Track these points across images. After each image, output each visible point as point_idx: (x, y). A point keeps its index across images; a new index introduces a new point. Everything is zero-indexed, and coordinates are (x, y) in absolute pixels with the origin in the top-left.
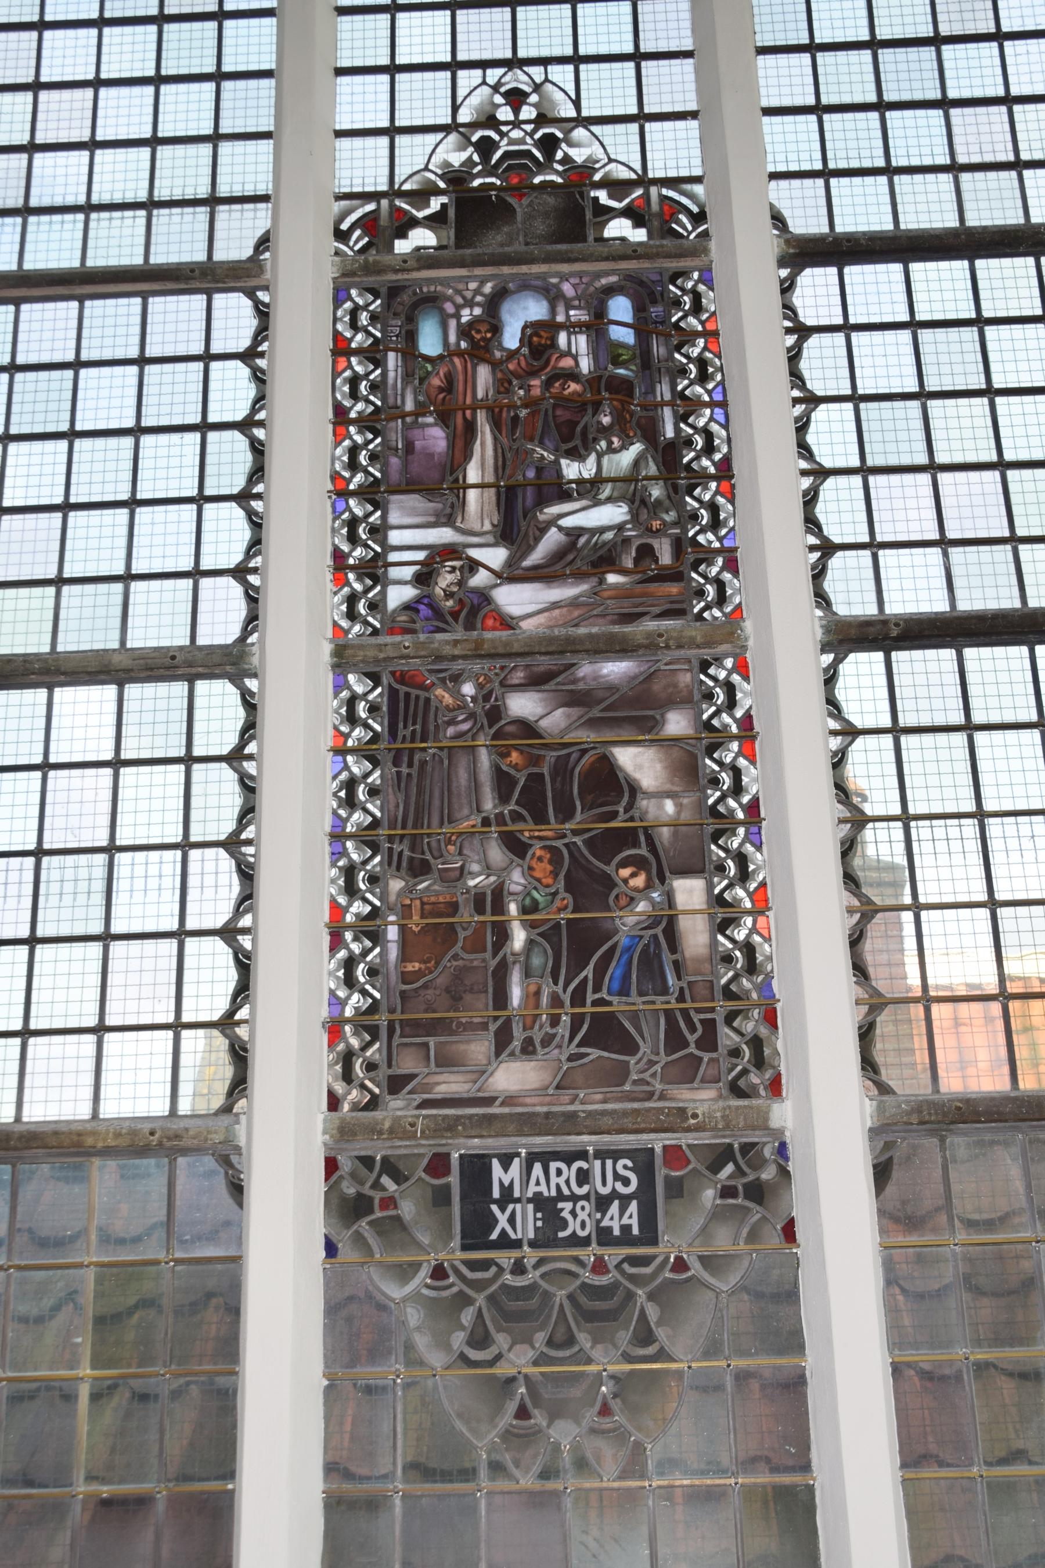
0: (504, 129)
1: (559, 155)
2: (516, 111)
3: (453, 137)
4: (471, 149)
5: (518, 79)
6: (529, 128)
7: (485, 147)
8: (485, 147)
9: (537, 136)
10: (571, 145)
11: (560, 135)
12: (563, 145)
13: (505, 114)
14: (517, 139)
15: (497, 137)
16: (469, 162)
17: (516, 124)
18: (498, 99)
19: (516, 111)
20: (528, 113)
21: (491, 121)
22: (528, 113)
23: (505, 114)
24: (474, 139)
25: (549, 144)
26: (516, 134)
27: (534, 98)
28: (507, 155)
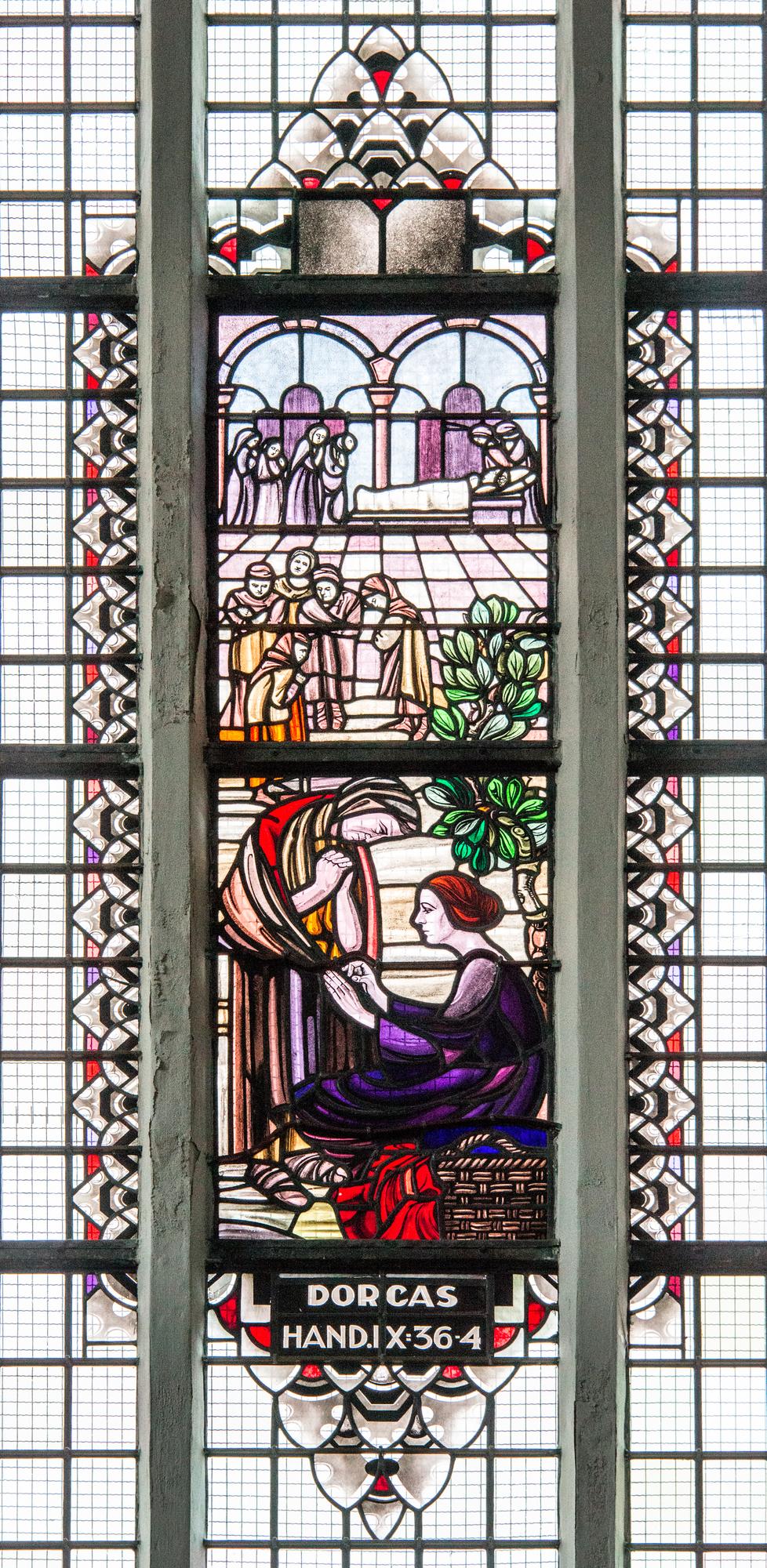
0: (368, 112)
1: (426, 151)
2: (382, 90)
3: (310, 119)
4: (333, 136)
5: (383, 40)
6: (396, 111)
7: (347, 134)
8: (347, 134)
9: (406, 123)
10: (441, 139)
11: (430, 122)
12: (431, 136)
13: (370, 94)
14: (383, 127)
15: (358, 122)
16: (326, 154)
17: (382, 106)
18: (362, 73)
19: (382, 90)
20: (395, 94)
21: (354, 101)
22: (395, 94)
23: (370, 94)
24: (335, 123)
25: (417, 133)
26: (382, 119)
27: (401, 73)
28: (370, 145)
